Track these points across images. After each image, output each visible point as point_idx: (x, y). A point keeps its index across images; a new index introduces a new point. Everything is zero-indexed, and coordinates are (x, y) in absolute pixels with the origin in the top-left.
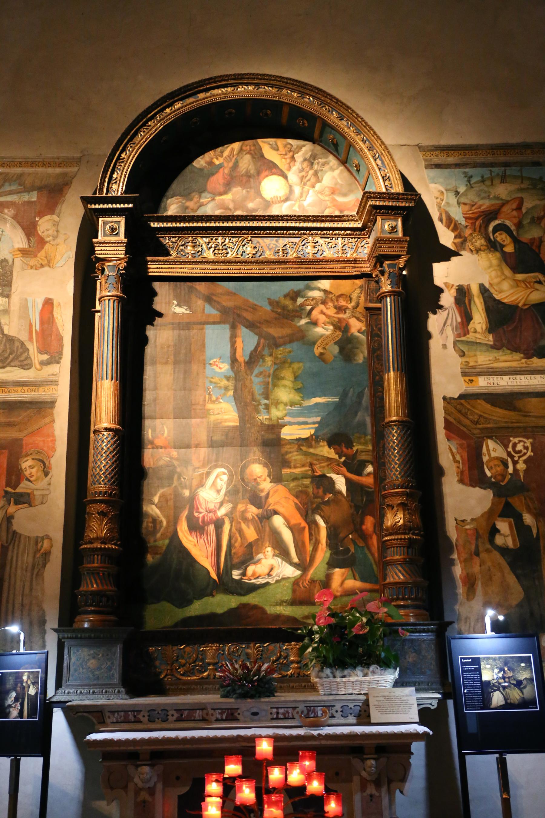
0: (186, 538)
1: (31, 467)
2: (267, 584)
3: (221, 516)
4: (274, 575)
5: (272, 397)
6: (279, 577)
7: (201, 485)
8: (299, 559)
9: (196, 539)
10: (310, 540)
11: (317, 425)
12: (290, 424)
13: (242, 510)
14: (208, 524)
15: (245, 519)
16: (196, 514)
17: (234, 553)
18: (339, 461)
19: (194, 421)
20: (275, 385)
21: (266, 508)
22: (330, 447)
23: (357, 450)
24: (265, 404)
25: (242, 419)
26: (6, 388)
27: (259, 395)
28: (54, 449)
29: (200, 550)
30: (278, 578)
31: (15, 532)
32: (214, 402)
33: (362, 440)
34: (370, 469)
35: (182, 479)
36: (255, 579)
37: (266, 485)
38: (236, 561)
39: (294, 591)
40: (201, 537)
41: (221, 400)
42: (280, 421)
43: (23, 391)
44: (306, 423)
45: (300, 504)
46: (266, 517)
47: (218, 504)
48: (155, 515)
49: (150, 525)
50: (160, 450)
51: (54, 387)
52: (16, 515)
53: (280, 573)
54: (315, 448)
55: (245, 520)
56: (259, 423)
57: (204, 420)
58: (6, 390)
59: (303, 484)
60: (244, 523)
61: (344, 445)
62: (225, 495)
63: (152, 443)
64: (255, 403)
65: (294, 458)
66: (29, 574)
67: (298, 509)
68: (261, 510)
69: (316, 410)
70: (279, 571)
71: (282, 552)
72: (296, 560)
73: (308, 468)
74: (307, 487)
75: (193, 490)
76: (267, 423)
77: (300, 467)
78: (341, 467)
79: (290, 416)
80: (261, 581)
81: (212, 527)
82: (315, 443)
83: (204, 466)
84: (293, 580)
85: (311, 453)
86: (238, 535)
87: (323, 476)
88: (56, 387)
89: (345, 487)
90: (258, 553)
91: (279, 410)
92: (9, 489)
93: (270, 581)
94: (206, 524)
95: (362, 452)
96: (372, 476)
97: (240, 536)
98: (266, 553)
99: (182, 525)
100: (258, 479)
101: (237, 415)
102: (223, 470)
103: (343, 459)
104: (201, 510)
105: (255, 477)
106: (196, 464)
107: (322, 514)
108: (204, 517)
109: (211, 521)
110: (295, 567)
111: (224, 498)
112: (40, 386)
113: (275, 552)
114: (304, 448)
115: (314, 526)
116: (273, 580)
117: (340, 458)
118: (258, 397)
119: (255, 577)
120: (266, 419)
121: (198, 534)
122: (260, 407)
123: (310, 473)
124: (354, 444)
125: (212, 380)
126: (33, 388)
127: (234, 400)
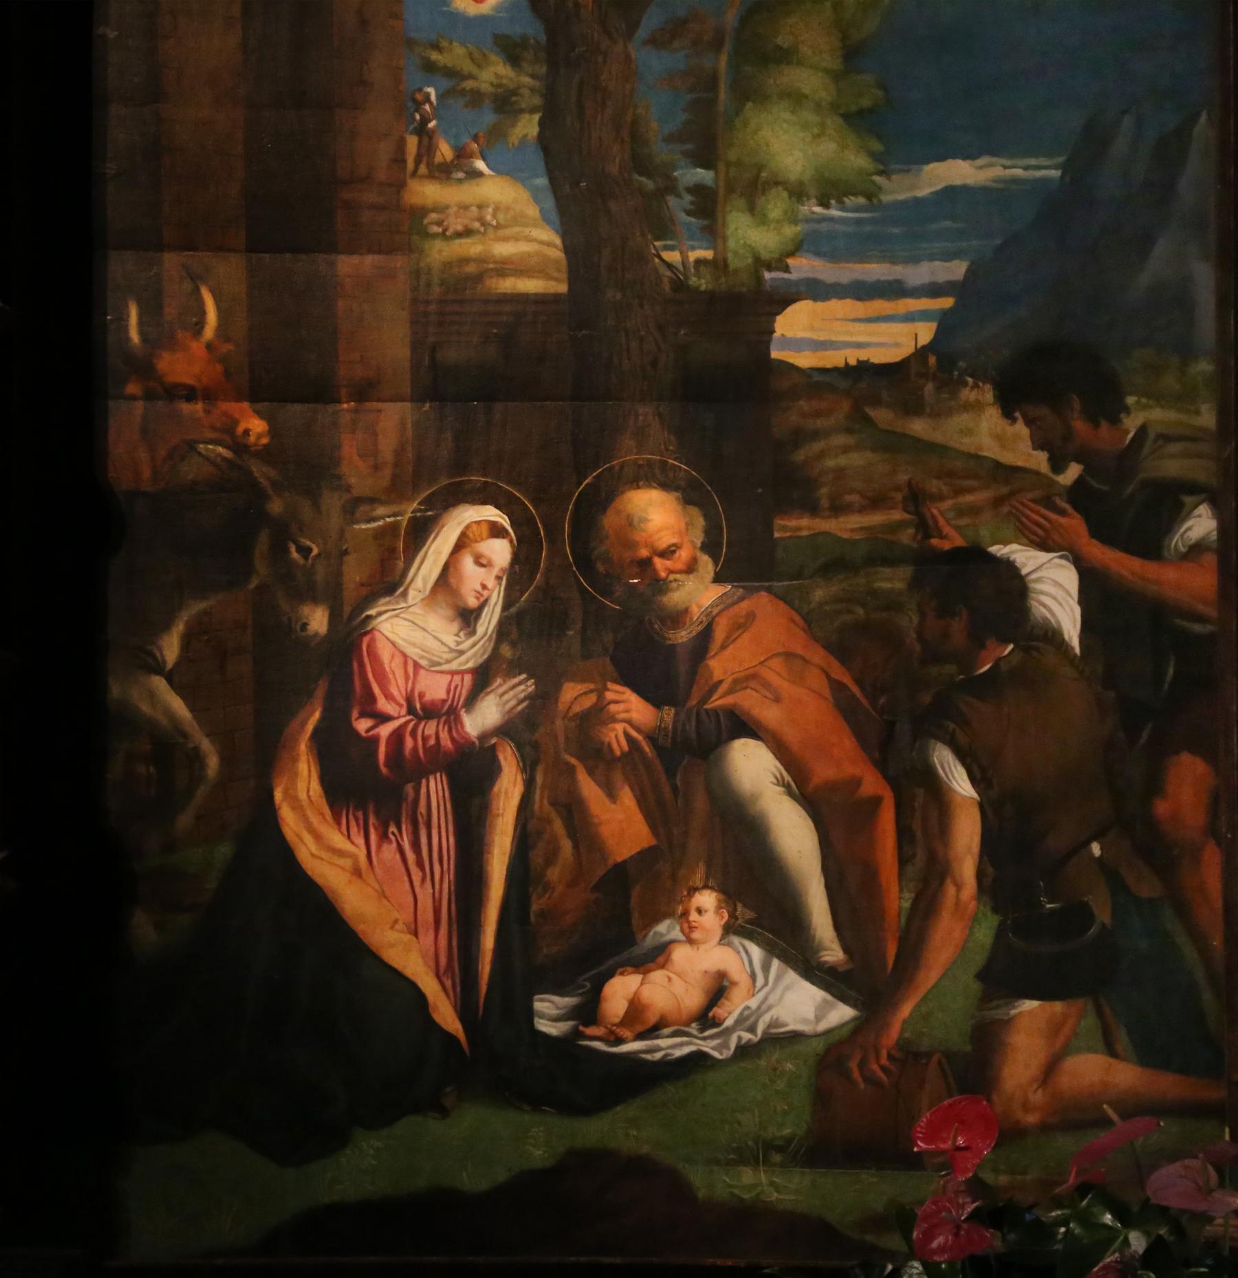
0: (318, 837)
2: (698, 1060)
3: (484, 737)
4: (729, 1022)
5: (732, 155)
6: (752, 1029)
7: (388, 583)
8: (846, 949)
9: (360, 841)
10: (903, 861)
11: (947, 302)
12: (817, 290)
13: (577, 709)
14: (420, 771)
15: (598, 758)
16: (362, 725)
17: (542, 914)
18: (1052, 483)
19: (346, 265)
20: (747, 93)
21: (693, 702)
22: (1008, 414)
23: (1142, 431)
24: (698, 190)
25: (580, 258)
27: (669, 139)
29: (383, 895)
30: (746, 1036)
32: (442, 173)
33: (1170, 382)
34: (1201, 524)
35: (295, 555)
36: (640, 1036)
37: (698, 593)
38: (548, 949)
39: (821, 1097)
40: (384, 837)
41: (480, 165)
42: (767, 275)
44: (895, 290)
45: (855, 689)
46: (693, 747)
47: (468, 678)
48: (164, 721)
49: (141, 769)
50: (185, 408)
53: (759, 1012)
54: (937, 415)
55: (598, 758)
56: (667, 287)
57: (399, 262)
59: (874, 593)
60: (591, 772)
61: (1077, 404)
62: (502, 632)
63: (143, 368)
64: (649, 184)
65: (830, 463)
67: (846, 707)
68: (669, 714)
69: (948, 223)
70: (753, 1003)
71: (767, 912)
72: (833, 954)
73: (897, 515)
74: (892, 604)
75: (347, 609)
76: (702, 283)
77: (862, 510)
78: (1062, 513)
79: (818, 254)
80: (671, 1047)
81: (436, 789)
82: (938, 389)
83: (396, 492)
84: (819, 1046)
85: (917, 441)
86: (558, 826)
87: (975, 556)
89: (1078, 610)
90: (658, 919)
91: (761, 220)
93: (708, 1047)
94: (408, 769)
95: (1166, 438)
96: (1210, 559)
97: (572, 833)
98: (694, 916)
99: (295, 775)
100: (659, 563)
101: (558, 241)
102: (490, 513)
103: (1073, 472)
104: (383, 705)
105: (644, 553)
106: (356, 473)
107: (961, 738)
108: (397, 737)
109: (435, 760)
110: (826, 987)
111: (496, 649)
113: (732, 915)
114: (882, 416)
115: (920, 793)
116: (725, 1045)
117: (1058, 465)
118: (661, 151)
119: (640, 1028)
120: (698, 262)
121: (372, 820)
122: (672, 201)
123: (907, 537)
124: (1130, 400)
125: (434, 56)
127: (541, 166)
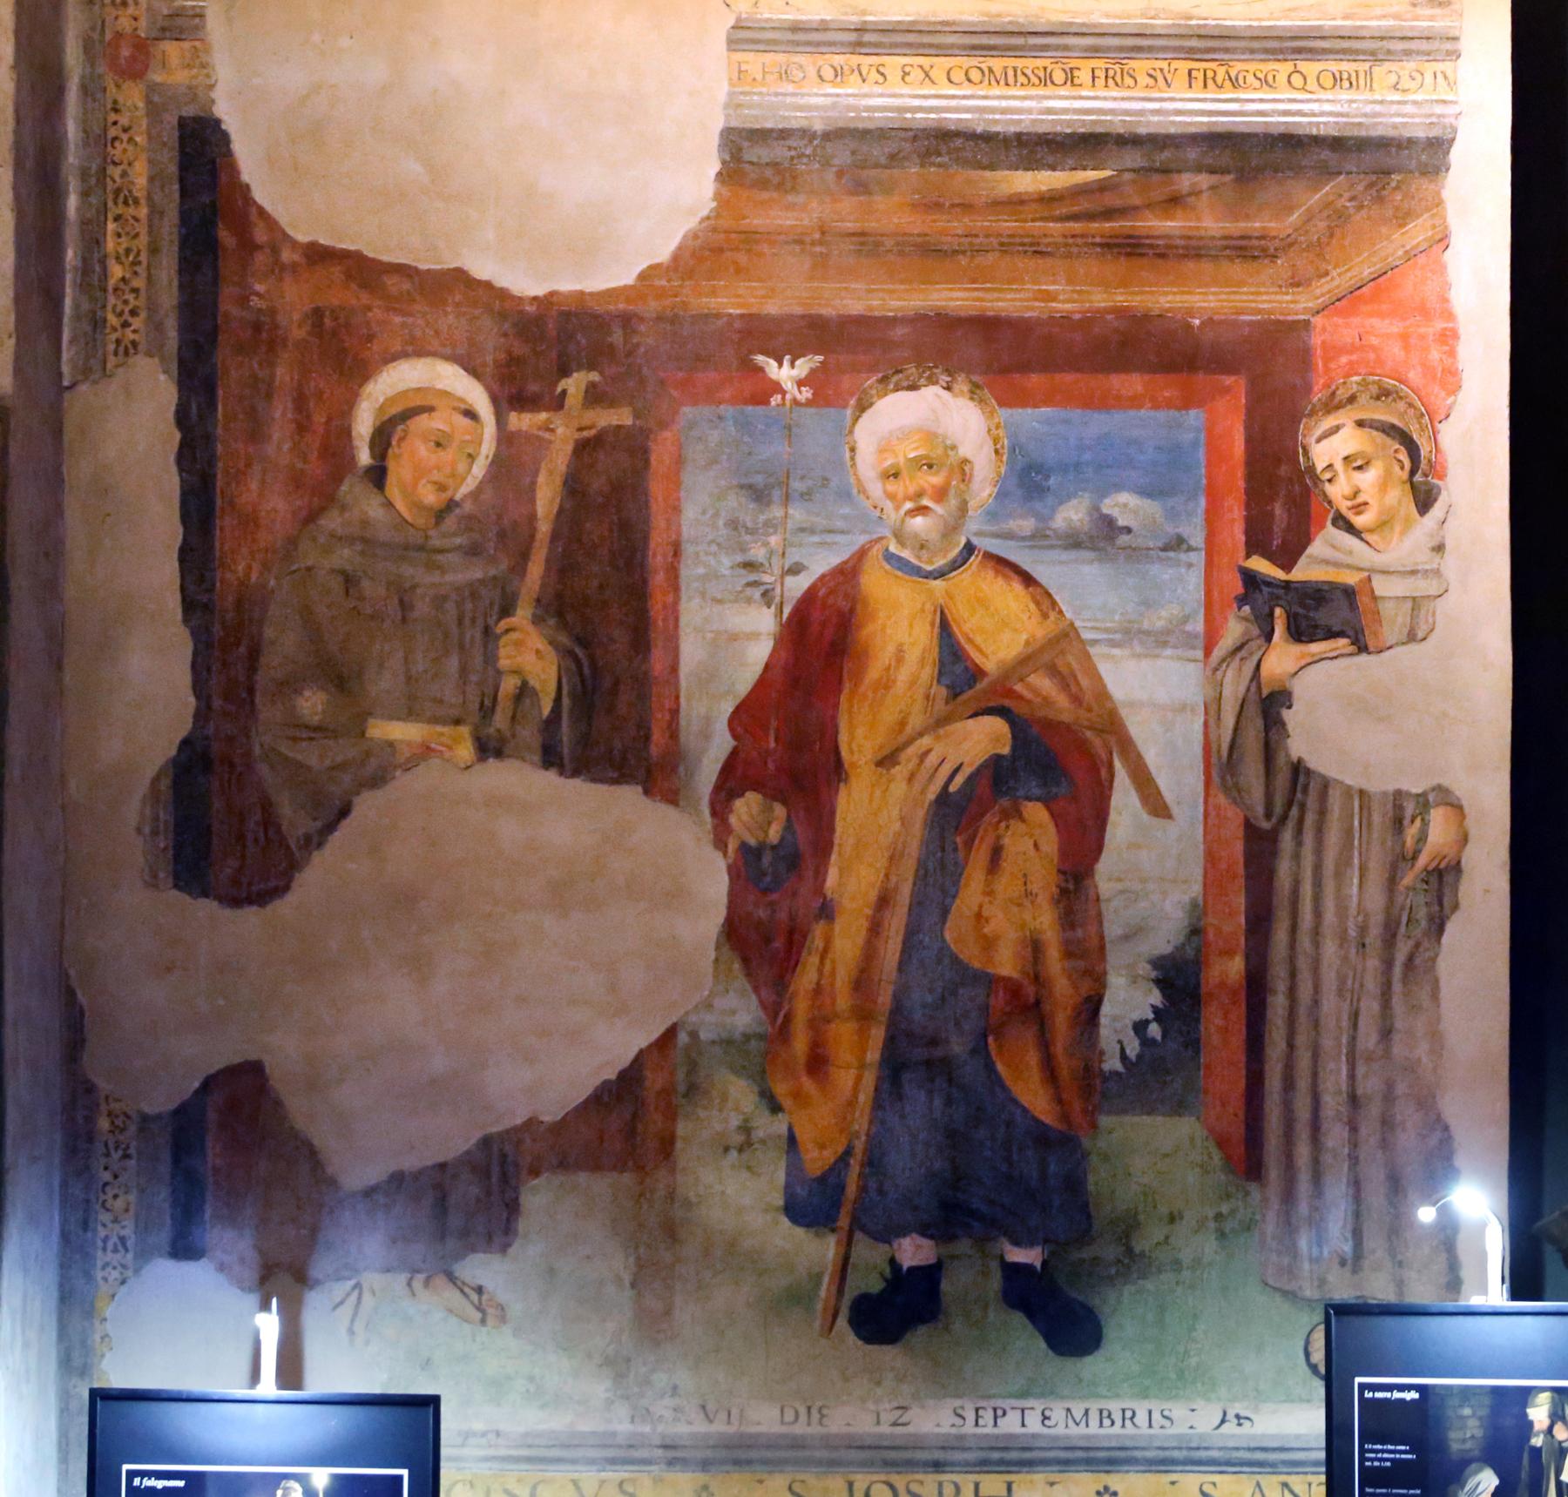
1: (1357, 463)
26: (1222, 63)
28: (1450, 379)
31: (1298, 769)
43: (1297, 80)
51: (1439, 66)
52: (1301, 689)
58: (1221, 72)
66: (1373, 963)
88: (1446, 66)
92: (1260, 565)
112: (1375, 57)
126: (1345, 66)
